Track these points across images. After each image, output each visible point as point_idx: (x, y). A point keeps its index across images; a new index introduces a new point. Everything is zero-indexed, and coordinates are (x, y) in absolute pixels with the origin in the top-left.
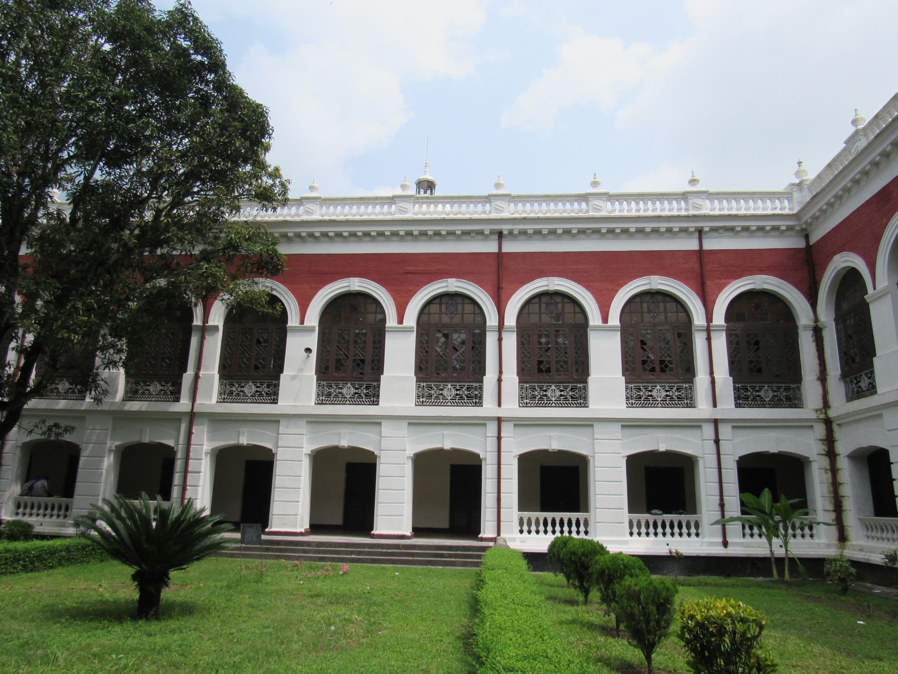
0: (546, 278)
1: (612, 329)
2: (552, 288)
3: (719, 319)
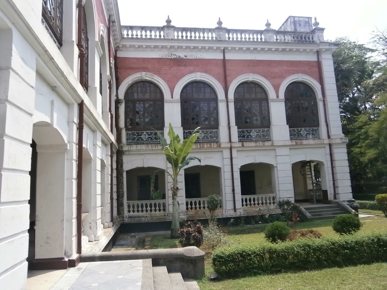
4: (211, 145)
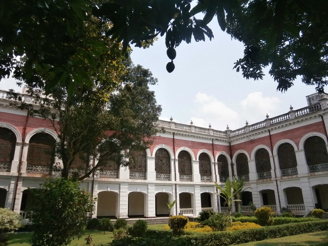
0: (184, 147)
1: (197, 162)
4: (267, 180)
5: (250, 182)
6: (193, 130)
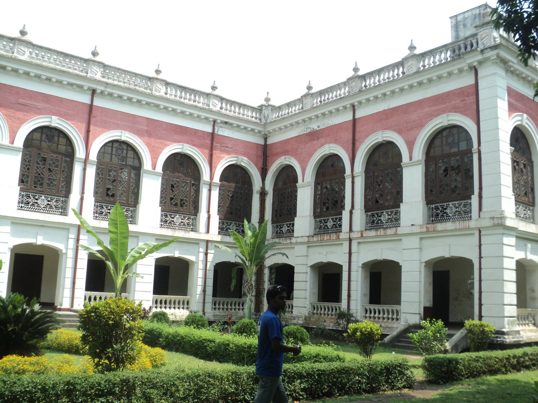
2: (123, 138)
3: (217, 179)
4: (330, 236)
5: (294, 240)
6: (160, 90)
